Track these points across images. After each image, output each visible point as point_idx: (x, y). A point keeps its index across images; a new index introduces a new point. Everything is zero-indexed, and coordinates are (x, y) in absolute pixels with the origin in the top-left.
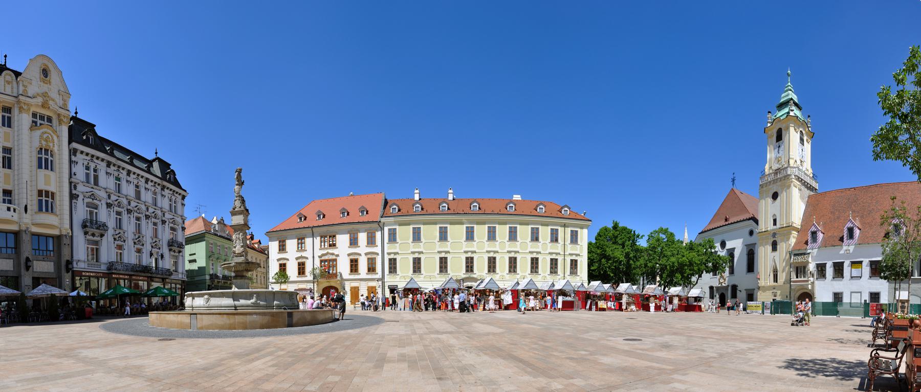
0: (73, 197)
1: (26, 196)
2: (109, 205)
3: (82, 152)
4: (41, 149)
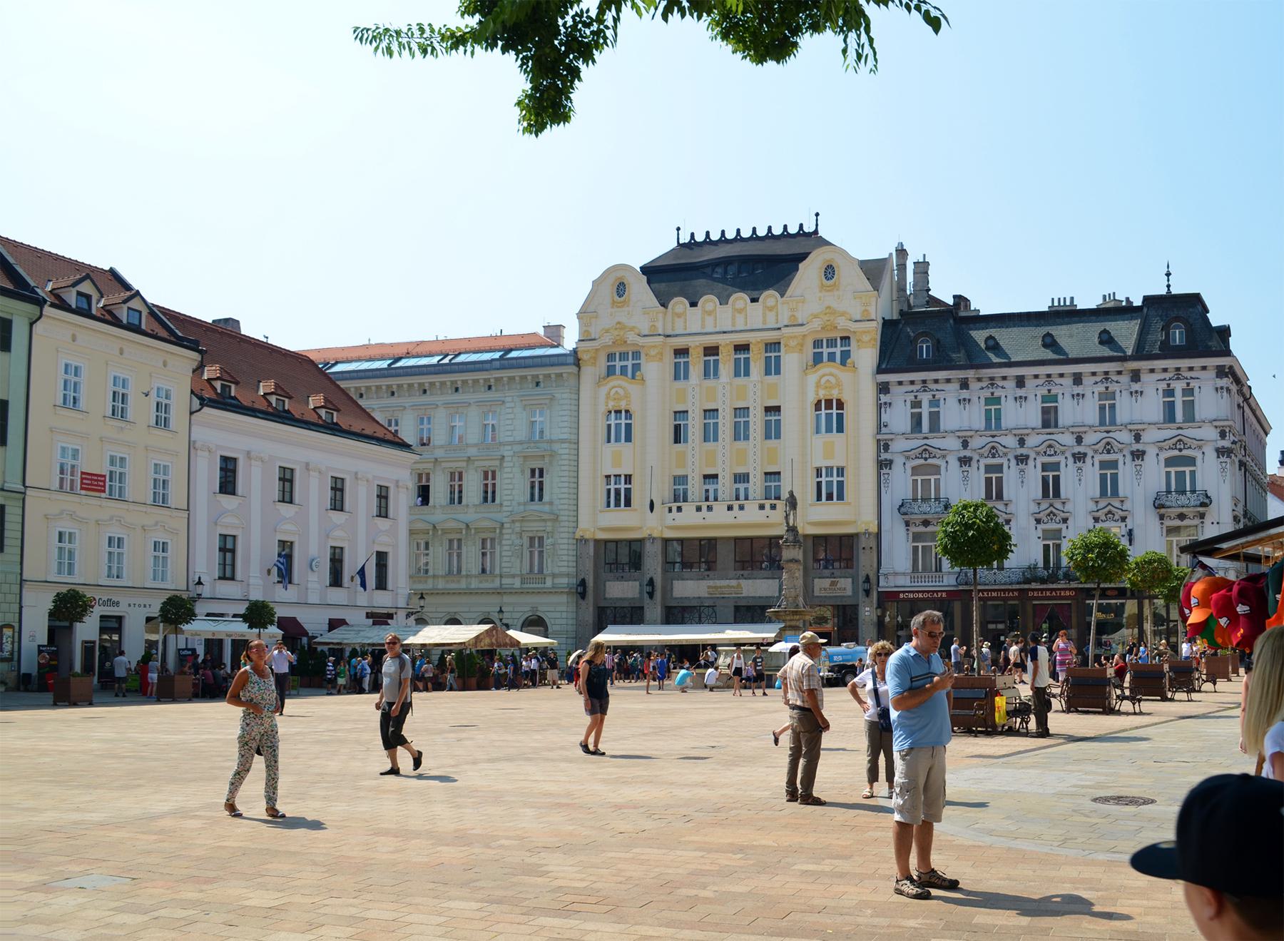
0: (883, 465)
2: (965, 461)
3: (900, 383)
4: (820, 401)
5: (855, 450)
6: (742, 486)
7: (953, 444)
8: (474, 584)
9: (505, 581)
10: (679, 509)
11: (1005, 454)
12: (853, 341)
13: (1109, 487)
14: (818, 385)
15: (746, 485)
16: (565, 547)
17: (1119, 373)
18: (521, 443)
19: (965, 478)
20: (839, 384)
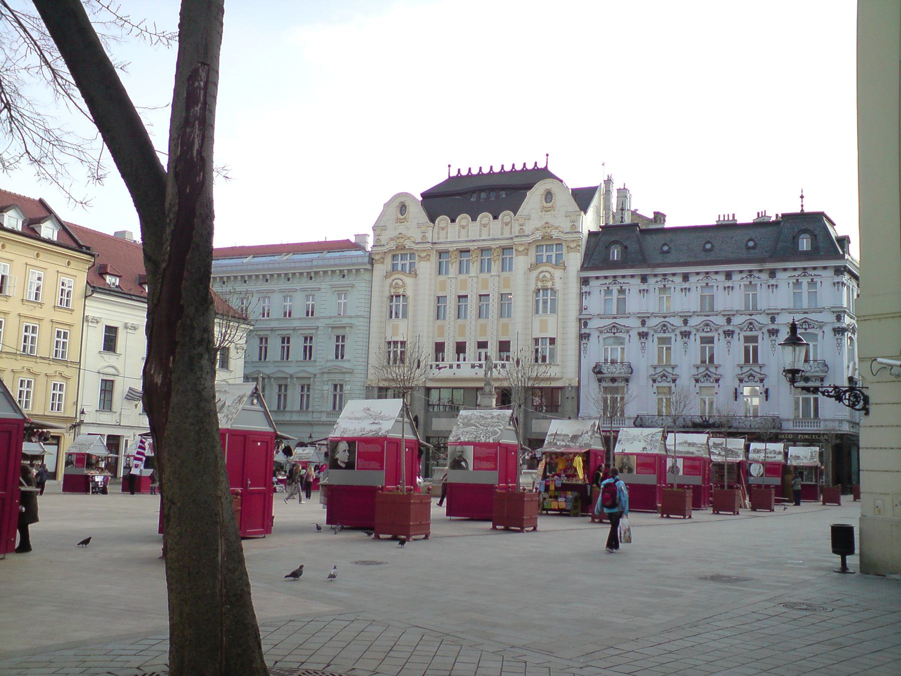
0: (583, 337)
1: (521, 348)
2: (643, 335)
3: (597, 278)
5: (561, 325)
6: (483, 351)
7: (634, 323)
8: (295, 418)
9: (315, 415)
10: (459, 366)
11: (673, 331)
12: (565, 248)
13: (751, 356)
14: (537, 279)
15: (485, 350)
16: (358, 392)
17: (760, 271)
18: (330, 317)
19: (643, 348)
20: (552, 278)
